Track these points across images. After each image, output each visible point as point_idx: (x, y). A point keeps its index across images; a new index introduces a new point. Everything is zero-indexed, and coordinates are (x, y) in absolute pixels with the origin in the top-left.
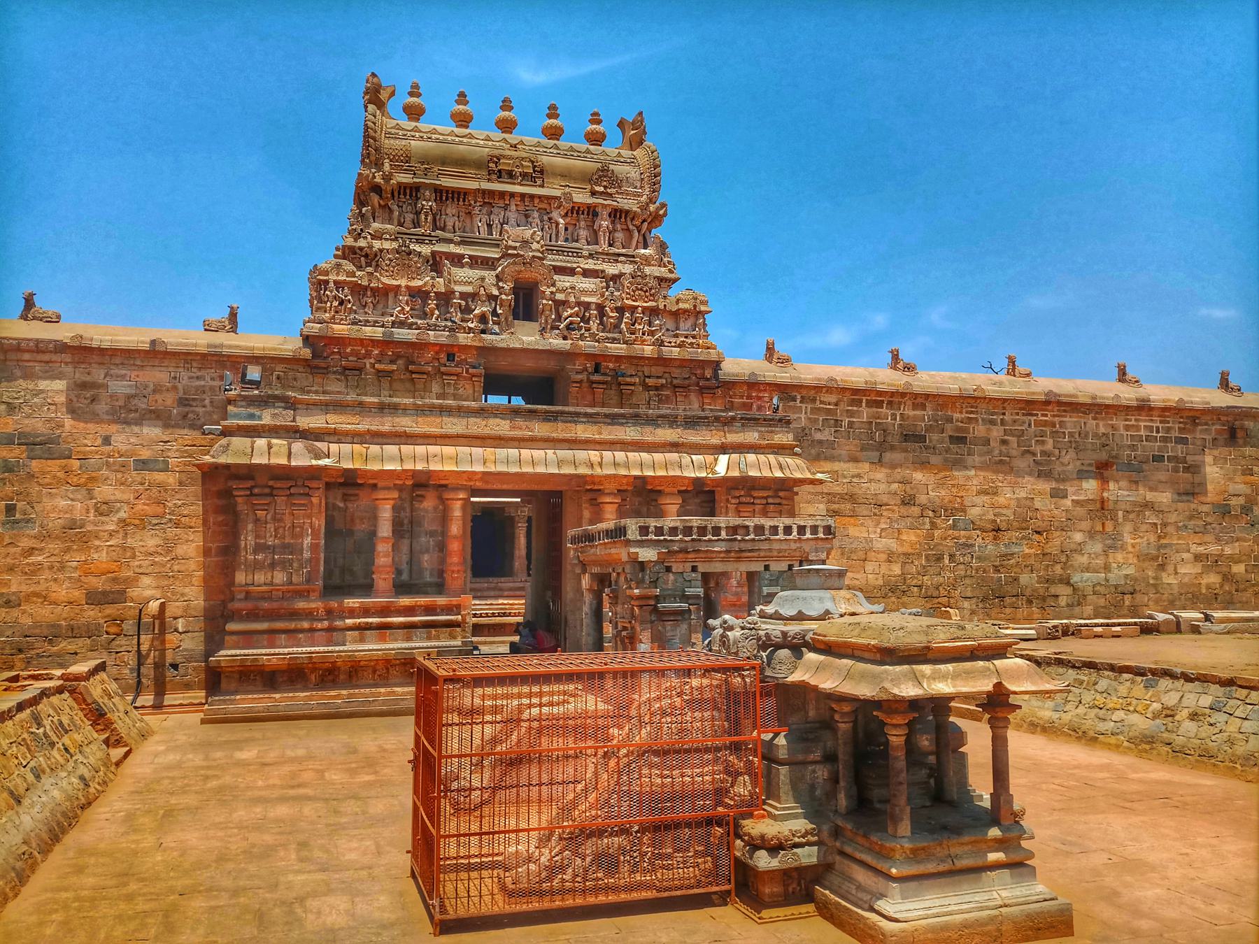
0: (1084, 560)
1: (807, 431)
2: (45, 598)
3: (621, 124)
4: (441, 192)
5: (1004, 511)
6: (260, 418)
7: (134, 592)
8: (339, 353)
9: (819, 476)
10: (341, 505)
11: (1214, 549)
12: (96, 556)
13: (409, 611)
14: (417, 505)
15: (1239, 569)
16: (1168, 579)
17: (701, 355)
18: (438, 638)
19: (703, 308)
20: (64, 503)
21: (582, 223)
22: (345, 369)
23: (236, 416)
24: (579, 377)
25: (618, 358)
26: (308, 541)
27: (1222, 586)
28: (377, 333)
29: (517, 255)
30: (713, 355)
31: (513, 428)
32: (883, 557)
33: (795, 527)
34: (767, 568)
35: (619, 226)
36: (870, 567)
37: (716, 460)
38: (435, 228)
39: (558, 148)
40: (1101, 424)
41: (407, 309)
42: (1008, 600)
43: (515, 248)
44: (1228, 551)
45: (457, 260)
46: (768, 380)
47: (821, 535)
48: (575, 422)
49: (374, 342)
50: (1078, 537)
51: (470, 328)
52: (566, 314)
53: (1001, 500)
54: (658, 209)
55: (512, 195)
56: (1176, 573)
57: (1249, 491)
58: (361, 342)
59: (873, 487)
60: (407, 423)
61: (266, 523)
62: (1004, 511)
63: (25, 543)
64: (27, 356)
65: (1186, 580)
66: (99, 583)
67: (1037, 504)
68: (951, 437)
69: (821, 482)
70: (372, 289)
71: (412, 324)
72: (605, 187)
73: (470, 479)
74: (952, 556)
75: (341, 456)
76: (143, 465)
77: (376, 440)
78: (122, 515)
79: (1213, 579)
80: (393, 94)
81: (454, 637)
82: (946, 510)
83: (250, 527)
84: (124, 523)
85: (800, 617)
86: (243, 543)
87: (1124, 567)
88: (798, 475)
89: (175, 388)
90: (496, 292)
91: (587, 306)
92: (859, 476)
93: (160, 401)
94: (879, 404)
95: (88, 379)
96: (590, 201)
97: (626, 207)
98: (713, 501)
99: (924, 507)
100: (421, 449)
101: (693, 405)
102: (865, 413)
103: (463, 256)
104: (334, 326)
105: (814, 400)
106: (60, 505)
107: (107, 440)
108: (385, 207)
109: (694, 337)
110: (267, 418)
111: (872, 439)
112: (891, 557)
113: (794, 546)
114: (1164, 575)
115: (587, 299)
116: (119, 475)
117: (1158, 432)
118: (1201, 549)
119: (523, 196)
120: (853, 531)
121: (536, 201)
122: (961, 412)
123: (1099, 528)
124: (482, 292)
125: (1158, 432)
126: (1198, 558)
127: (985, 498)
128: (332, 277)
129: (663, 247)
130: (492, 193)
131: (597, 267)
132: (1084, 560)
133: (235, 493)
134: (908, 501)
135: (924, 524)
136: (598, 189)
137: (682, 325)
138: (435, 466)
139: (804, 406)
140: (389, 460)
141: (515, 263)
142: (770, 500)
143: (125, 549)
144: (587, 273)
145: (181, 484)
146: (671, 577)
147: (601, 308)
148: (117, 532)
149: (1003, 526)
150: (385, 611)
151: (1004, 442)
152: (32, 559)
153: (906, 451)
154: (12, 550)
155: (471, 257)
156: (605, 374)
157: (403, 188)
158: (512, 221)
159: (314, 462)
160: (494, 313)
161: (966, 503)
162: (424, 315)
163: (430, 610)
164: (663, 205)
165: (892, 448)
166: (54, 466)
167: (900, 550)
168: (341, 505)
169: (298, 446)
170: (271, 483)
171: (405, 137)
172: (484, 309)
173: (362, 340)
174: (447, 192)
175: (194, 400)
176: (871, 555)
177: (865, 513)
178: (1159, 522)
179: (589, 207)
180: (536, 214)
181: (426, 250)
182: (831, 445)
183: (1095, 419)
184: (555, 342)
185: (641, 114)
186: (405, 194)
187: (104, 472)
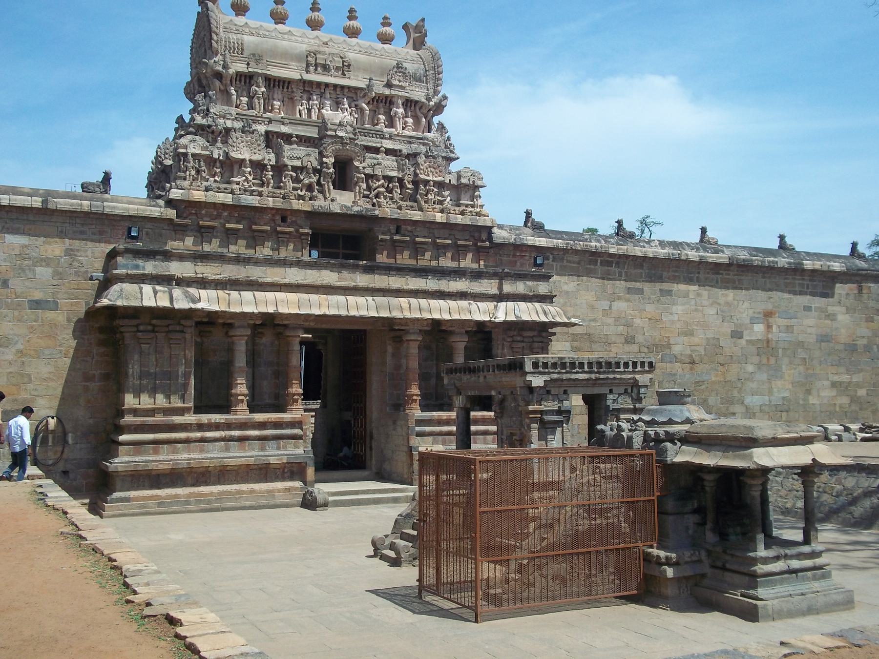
0: (754, 385)
3: (406, 27)
4: (270, 80)
6: (144, 268)
8: (196, 214)
9: (574, 320)
11: (845, 378)
13: (262, 425)
14: (257, 340)
15: (862, 392)
16: (813, 400)
18: (285, 448)
19: (479, 183)
23: (126, 267)
25: (415, 223)
26: (181, 369)
27: (850, 406)
28: (228, 199)
31: (340, 279)
37: (496, 307)
40: (768, 281)
41: (250, 178)
44: (855, 379)
46: (530, 243)
47: (647, 368)
48: (389, 275)
49: (224, 206)
50: (750, 368)
53: (696, 340)
55: (327, 85)
56: (819, 396)
57: (870, 334)
58: (214, 205)
61: (149, 354)
62: (698, 348)
65: (825, 401)
67: (722, 343)
69: (574, 325)
73: (306, 321)
75: (209, 301)
76: (37, 304)
77: (234, 287)
78: (20, 346)
79: (844, 400)
81: (296, 447)
83: (136, 357)
85: (670, 422)
86: (131, 371)
87: (782, 389)
88: (558, 320)
91: (389, 179)
92: (595, 320)
93: (50, 251)
94: (609, 264)
97: (416, 99)
100: (270, 295)
103: (291, 136)
105: (562, 259)
113: (630, 376)
114: (810, 398)
116: (16, 313)
117: (808, 288)
118: (836, 378)
121: (346, 90)
122: (668, 271)
123: (765, 361)
125: (808, 288)
126: (834, 385)
132: (754, 385)
133: (122, 329)
139: (555, 264)
140: (248, 303)
142: (536, 339)
143: (22, 375)
148: (16, 361)
149: (697, 359)
150: (243, 425)
153: (628, 300)
155: (297, 136)
156: (404, 235)
157: (239, 75)
159: (193, 306)
161: (672, 342)
163: (278, 425)
165: (619, 298)
169: (177, 292)
170: (154, 322)
173: (215, 204)
174: (275, 80)
175: (78, 250)
177: (599, 349)
178: (807, 357)
179: (387, 97)
183: (764, 277)
185: (423, 20)
186: (240, 81)
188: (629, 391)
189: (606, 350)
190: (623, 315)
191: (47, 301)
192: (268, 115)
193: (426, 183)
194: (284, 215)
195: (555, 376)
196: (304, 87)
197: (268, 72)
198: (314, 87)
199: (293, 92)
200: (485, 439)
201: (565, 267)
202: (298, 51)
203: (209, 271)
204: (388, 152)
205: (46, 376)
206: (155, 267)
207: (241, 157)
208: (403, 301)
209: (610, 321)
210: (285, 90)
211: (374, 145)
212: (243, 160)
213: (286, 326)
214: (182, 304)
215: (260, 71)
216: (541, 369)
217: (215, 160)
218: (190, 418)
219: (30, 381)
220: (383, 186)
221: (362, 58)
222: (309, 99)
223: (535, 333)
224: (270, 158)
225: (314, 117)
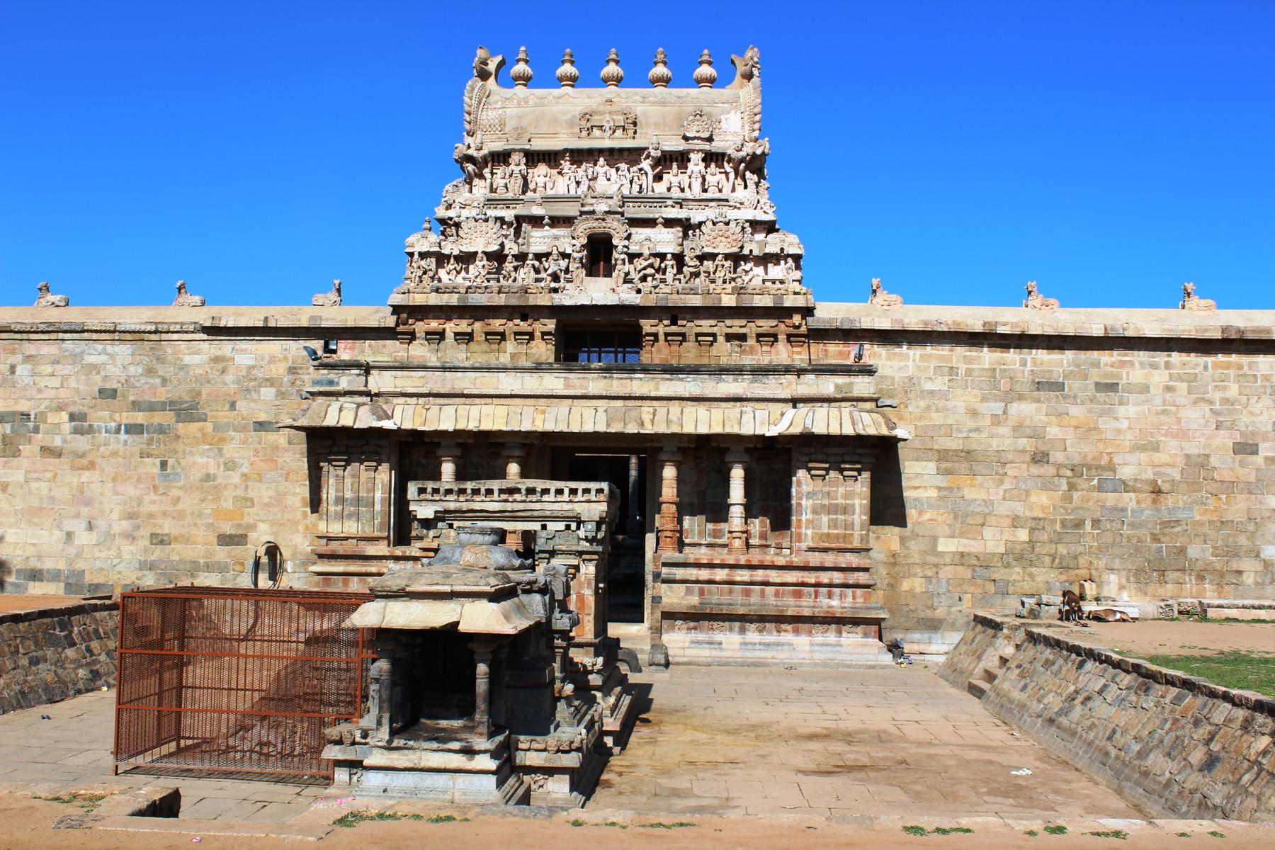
1: (915, 380)
2: (187, 540)
5: (1168, 470)
6: (338, 384)
7: (252, 536)
10: (424, 462)
12: (224, 505)
20: (201, 460)
22: (427, 333)
24: (653, 330)
28: (453, 300)
29: (593, 212)
30: (800, 302)
31: (567, 386)
32: (1009, 521)
33: (566, 491)
34: (544, 527)
36: (988, 533)
42: (1171, 575)
45: (537, 221)
53: (1162, 457)
59: (995, 444)
60: (465, 382)
63: (175, 493)
64: (175, 336)
66: (228, 529)
68: (1097, 384)
70: (455, 257)
71: (486, 287)
74: (1096, 522)
75: (404, 417)
76: (261, 426)
78: (244, 470)
82: (1089, 469)
83: (331, 481)
84: (244, 475)
89: (286, 358)
90: (569, 251)
91: (662, 256)
92: (977, 430)
95: (219, 353)
96: (680, 146)
98: (790, 460)
99: (1059, 466)
100: (475, 410)
101: (782, 353)
102: (987, 356)
103: (542, 218)
106: (201, 461)
107: (233, 406)
110: (346, 381)
111: (995, 388)
112: (1016, 522)
113: (566, 507)
115: (663, 251)
116: (242, 435)
119: (611, 151)
120: (969, 494)
121: (626, 154)
124: (555, 252)
127: (1144, 457)
131: (679, 217)
134: (1039, 458)
135: (1058, 486)
138: (486, 426)
139: (911, 352)
140: (445, 419)
143: (246, 499)
144: (669, 223)
145: (290, 443)
146: (453, 533)
147: (679, 259)
151: (1169, 389)
152: (180, 506)
153: (1039, 401)
154: (163, 497)
155: (551, 218)
160: (567, 271)
161: (1116, 460)
165: (1021, 398)
166: (194, 427)
167: (1028, 514)
168: (424, 462)
170: (346, 442)
172: (556, 268)
176: (991, 520)
181: (509, 215)
182: (943, 395)
184: (627, 296)
187: (231, 433)
188: (574, 526)
189: (997, 473)
190: (1028, 422)
191: (270, 423)
193: (713, 257)
194: (525, 312)
195: (452, 506)
197: (527, 147)
200: (763, 592)
201: (930, 356)
203: (410, 381)
204: (669, 223)
205: (267, 500)
206: (349, 382)
208: (646, 410)
209: (1004, 430)
211: (651, 216)
212: (476, 253)
213: (502, 445)
214: (366, 420)
216: (429, 497)
217: (448, 257)
218: (381, 549)
219: (253, 505)
220: (651, 266)
223: (842, 450)
225: (584, 187)
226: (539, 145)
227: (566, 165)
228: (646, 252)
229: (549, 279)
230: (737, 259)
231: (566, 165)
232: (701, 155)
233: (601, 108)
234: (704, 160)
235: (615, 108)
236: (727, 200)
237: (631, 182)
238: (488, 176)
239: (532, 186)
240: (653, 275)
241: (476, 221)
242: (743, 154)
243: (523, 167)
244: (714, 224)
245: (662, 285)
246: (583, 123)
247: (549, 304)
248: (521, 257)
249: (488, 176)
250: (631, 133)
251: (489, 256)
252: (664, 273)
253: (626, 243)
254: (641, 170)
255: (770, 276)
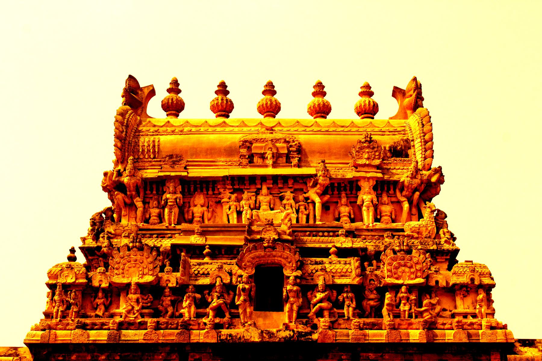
3: (397, 92)
17: (485, 336)
21: (344, 200)
28: (100, 336)
29: (262, 240)
30: (499, 337)
35: (385, 199)
38: (181, 219)
39: (319, 126)
43: (259, 233)
51: (205, 324)
52: (315, 300)
54: (430, 176)
55: (264, 178)
70: (104, 289)
72: (368, 159)
80: (152, 93)
91: (340, 288)
96: (350, 174)
103: (203, 247)
104: (59, 332)
108: (131, 206)
109: (474, 316)
115: (339, 281)
119: (275, 178)
121: (290, 182)
128: (61, 280)
129: (440, 218)
130: (241, 179)
131: (354, 246)
136: (360, 162)
137: (459, 302)
141: (255, 248)
144: (343, 253)
147: (358, 291)
158: (264, 206)
162: (156, 314)
164: (439, 170)
171: (157, 133)
180: (288, 194)
181: (166, 243)
186: (152, 191)
192: (184, 226)
193: (396, 288)
196: (233, 185)
198: (247, 182)
199: (220, 193)
202: (228, 143)
204: (343, 253)
207: (125, 281)
210: (210, 192)
211: (323, 246)
212: (129, 284)
215: (173, 174)
221: (319, 138)
222: (239, 200)
224: (173, 279)
226: (195, 172)
227: (226, 196)
228: (320, 282)
229: (211, 313)
230: (423, 291)
231: (226, 196)
232: (372, 183)
233: (264, 136)
234: (375, 188)
235: (277, 136)
236: (403, 230)
237: (298, 211)
238: (139, 203)
239: (188, 216)
240: (330, 310)
241: (129, 249)
242: (417, 181)
243: (179, 195)
244: (395, 252)
245: (341, 321)
246: (244, 151)
247: (214, 341)
248: (180, 291)
249: (139, 203)
250: (295, 161)
251: (142, 288)
252: (341, 306)
253: (299, 273)
254: (307, 199)
255: (461, 309)
